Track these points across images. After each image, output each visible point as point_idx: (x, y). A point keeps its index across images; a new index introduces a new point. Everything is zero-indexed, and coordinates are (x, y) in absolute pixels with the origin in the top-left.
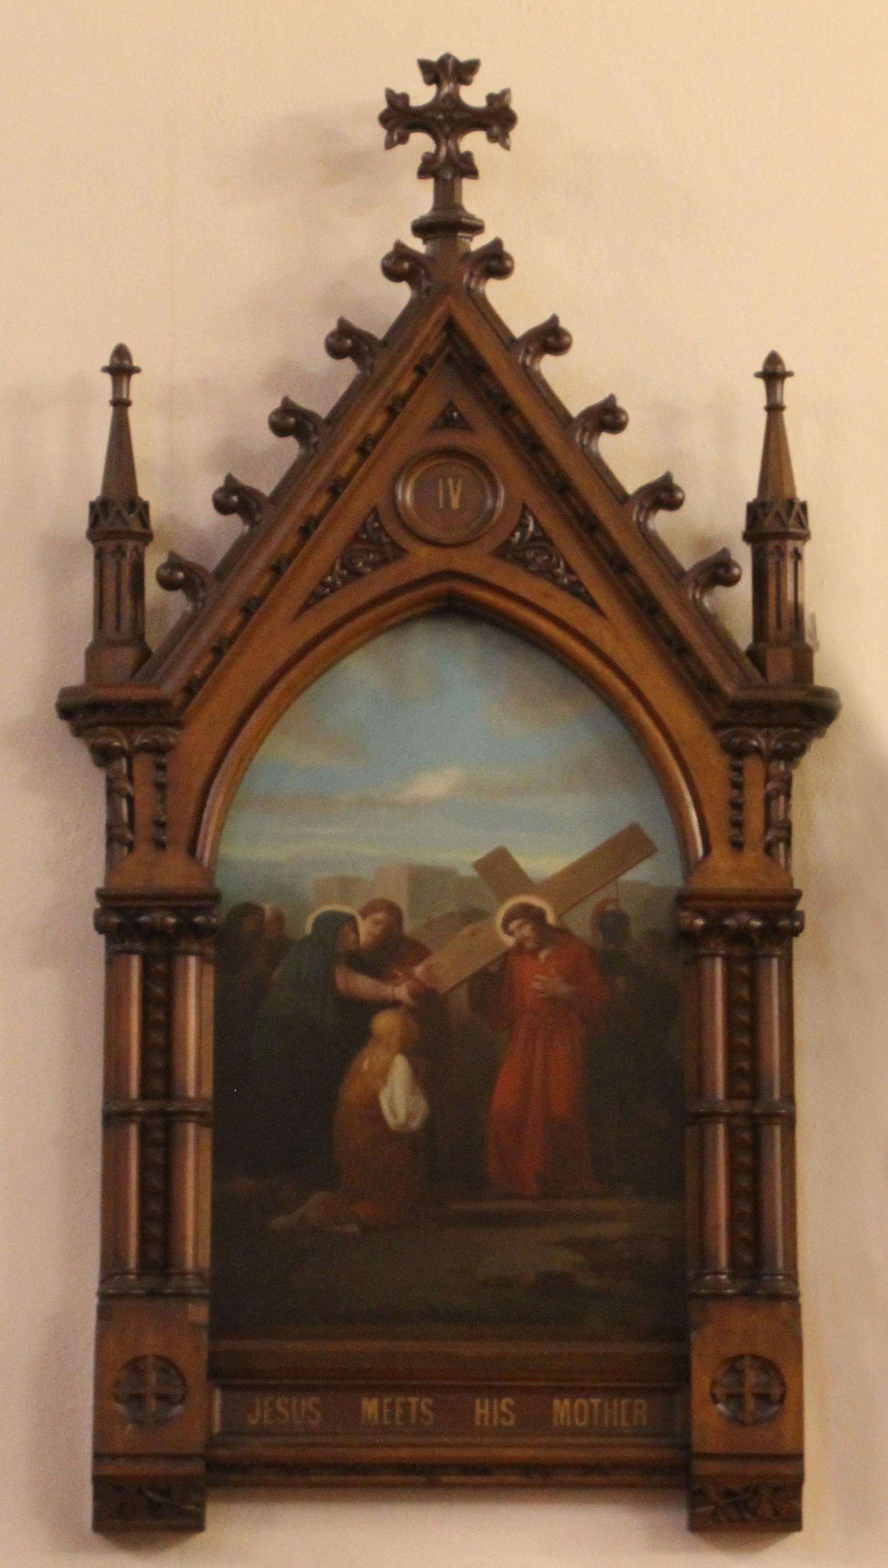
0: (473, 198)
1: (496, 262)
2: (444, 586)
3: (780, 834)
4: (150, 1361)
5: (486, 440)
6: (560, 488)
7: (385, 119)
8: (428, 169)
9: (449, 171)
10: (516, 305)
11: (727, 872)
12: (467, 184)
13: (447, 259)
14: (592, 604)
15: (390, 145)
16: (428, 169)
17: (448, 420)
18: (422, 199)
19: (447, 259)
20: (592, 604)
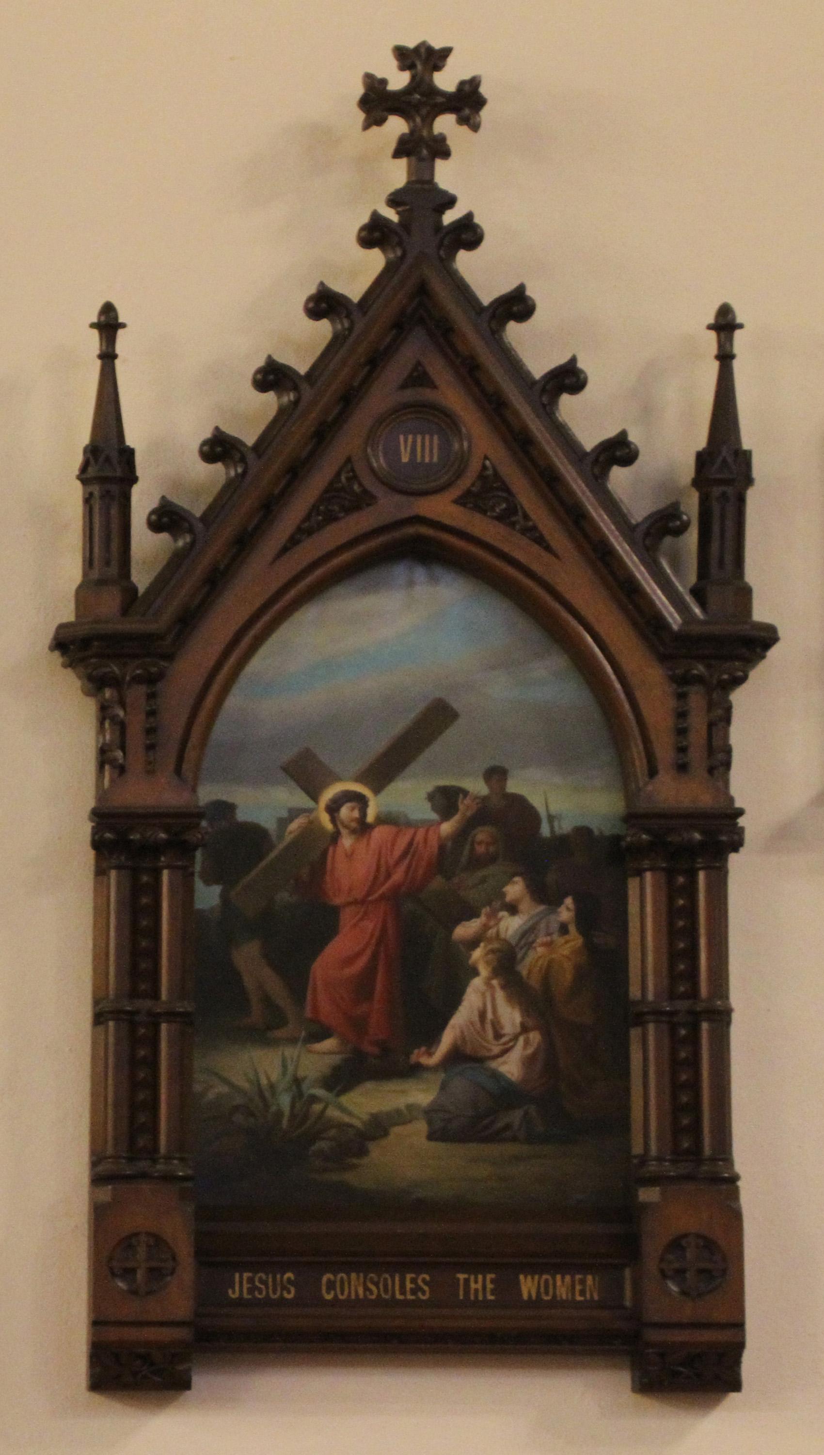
0: (445, 175)
1: (468, 234)
2: (424, 530)
3: (719, 760)
4: (143, 1238)
5: (452, 395)
6: (521, 443)
7: (365, 103)
8: (404, 148)
9: (421, 149)
10: (483, 273)
11: (670, 792)
12: (439, 164)
13: (421, 232)
14: (540, 540)
15: (367, 126)
16: (404, 148)
17: (419, 378)
18: (398, 174)
19: (421, 232)
20: (540, 540)
